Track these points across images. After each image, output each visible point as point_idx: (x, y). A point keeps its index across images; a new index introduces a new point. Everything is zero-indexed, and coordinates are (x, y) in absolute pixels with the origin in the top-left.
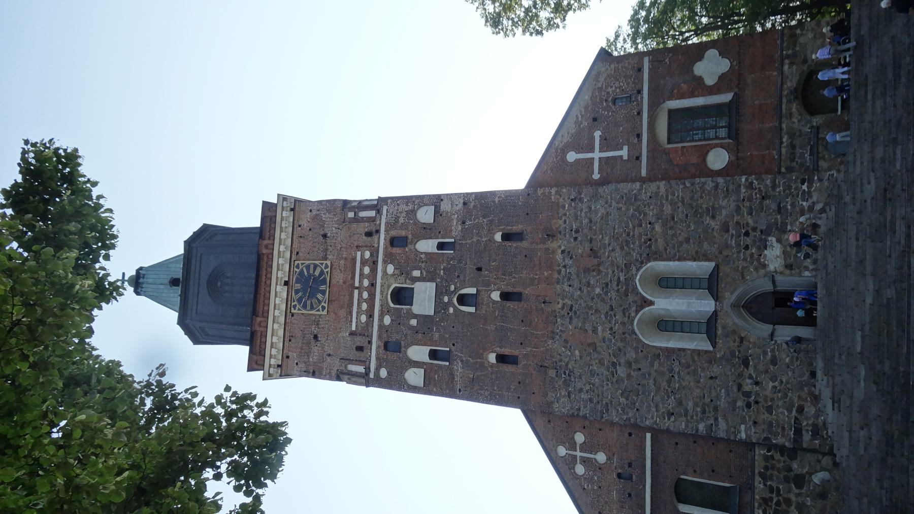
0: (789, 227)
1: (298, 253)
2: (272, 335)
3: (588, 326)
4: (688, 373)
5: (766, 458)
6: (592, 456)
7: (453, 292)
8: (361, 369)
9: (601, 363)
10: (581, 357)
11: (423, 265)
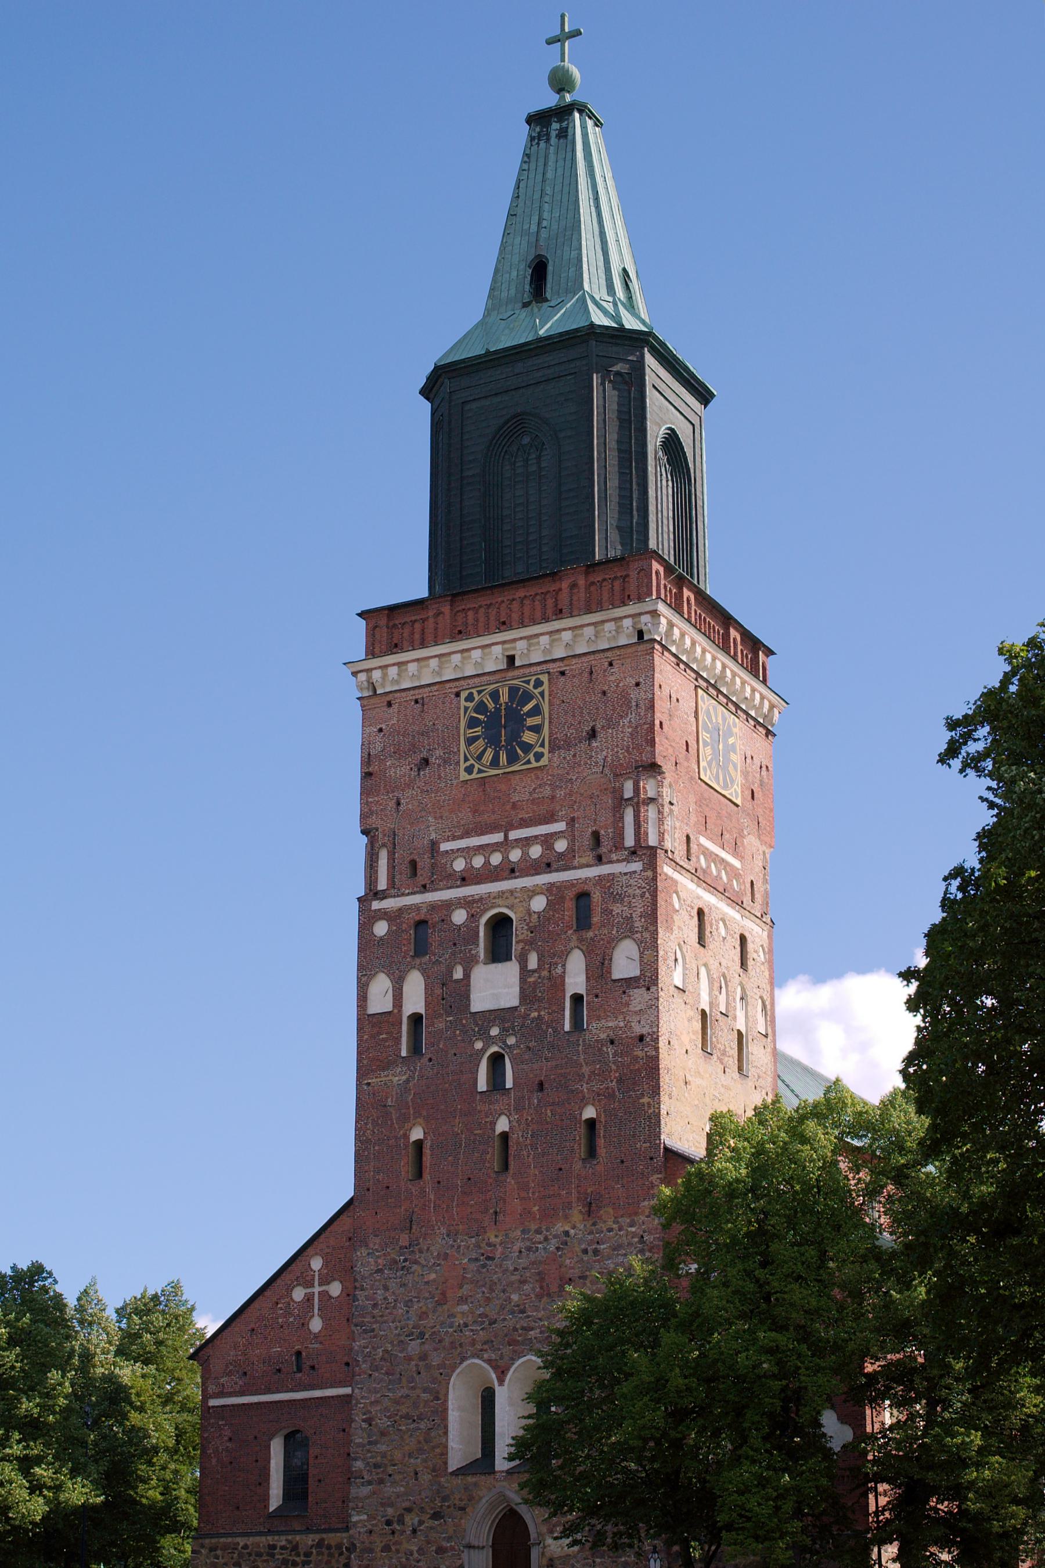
0: (598, 1560)
1: (563, 673)
2: (418, 660)
3: (466, 1290)
4: (419, 1442)
5: (339, 1546)
6: (316, 1311)
7: (504, 1042)
8: (382, 884)
9: (423, 1315)
10: (427, 1283)
11: (545, 973)
